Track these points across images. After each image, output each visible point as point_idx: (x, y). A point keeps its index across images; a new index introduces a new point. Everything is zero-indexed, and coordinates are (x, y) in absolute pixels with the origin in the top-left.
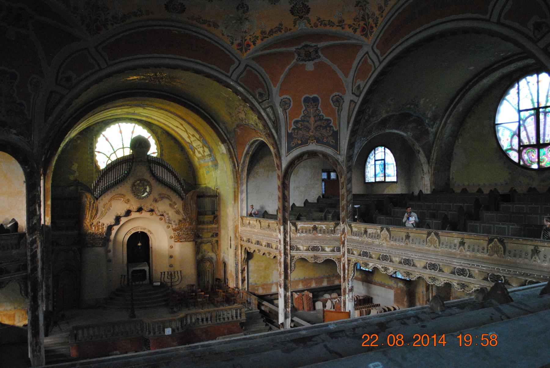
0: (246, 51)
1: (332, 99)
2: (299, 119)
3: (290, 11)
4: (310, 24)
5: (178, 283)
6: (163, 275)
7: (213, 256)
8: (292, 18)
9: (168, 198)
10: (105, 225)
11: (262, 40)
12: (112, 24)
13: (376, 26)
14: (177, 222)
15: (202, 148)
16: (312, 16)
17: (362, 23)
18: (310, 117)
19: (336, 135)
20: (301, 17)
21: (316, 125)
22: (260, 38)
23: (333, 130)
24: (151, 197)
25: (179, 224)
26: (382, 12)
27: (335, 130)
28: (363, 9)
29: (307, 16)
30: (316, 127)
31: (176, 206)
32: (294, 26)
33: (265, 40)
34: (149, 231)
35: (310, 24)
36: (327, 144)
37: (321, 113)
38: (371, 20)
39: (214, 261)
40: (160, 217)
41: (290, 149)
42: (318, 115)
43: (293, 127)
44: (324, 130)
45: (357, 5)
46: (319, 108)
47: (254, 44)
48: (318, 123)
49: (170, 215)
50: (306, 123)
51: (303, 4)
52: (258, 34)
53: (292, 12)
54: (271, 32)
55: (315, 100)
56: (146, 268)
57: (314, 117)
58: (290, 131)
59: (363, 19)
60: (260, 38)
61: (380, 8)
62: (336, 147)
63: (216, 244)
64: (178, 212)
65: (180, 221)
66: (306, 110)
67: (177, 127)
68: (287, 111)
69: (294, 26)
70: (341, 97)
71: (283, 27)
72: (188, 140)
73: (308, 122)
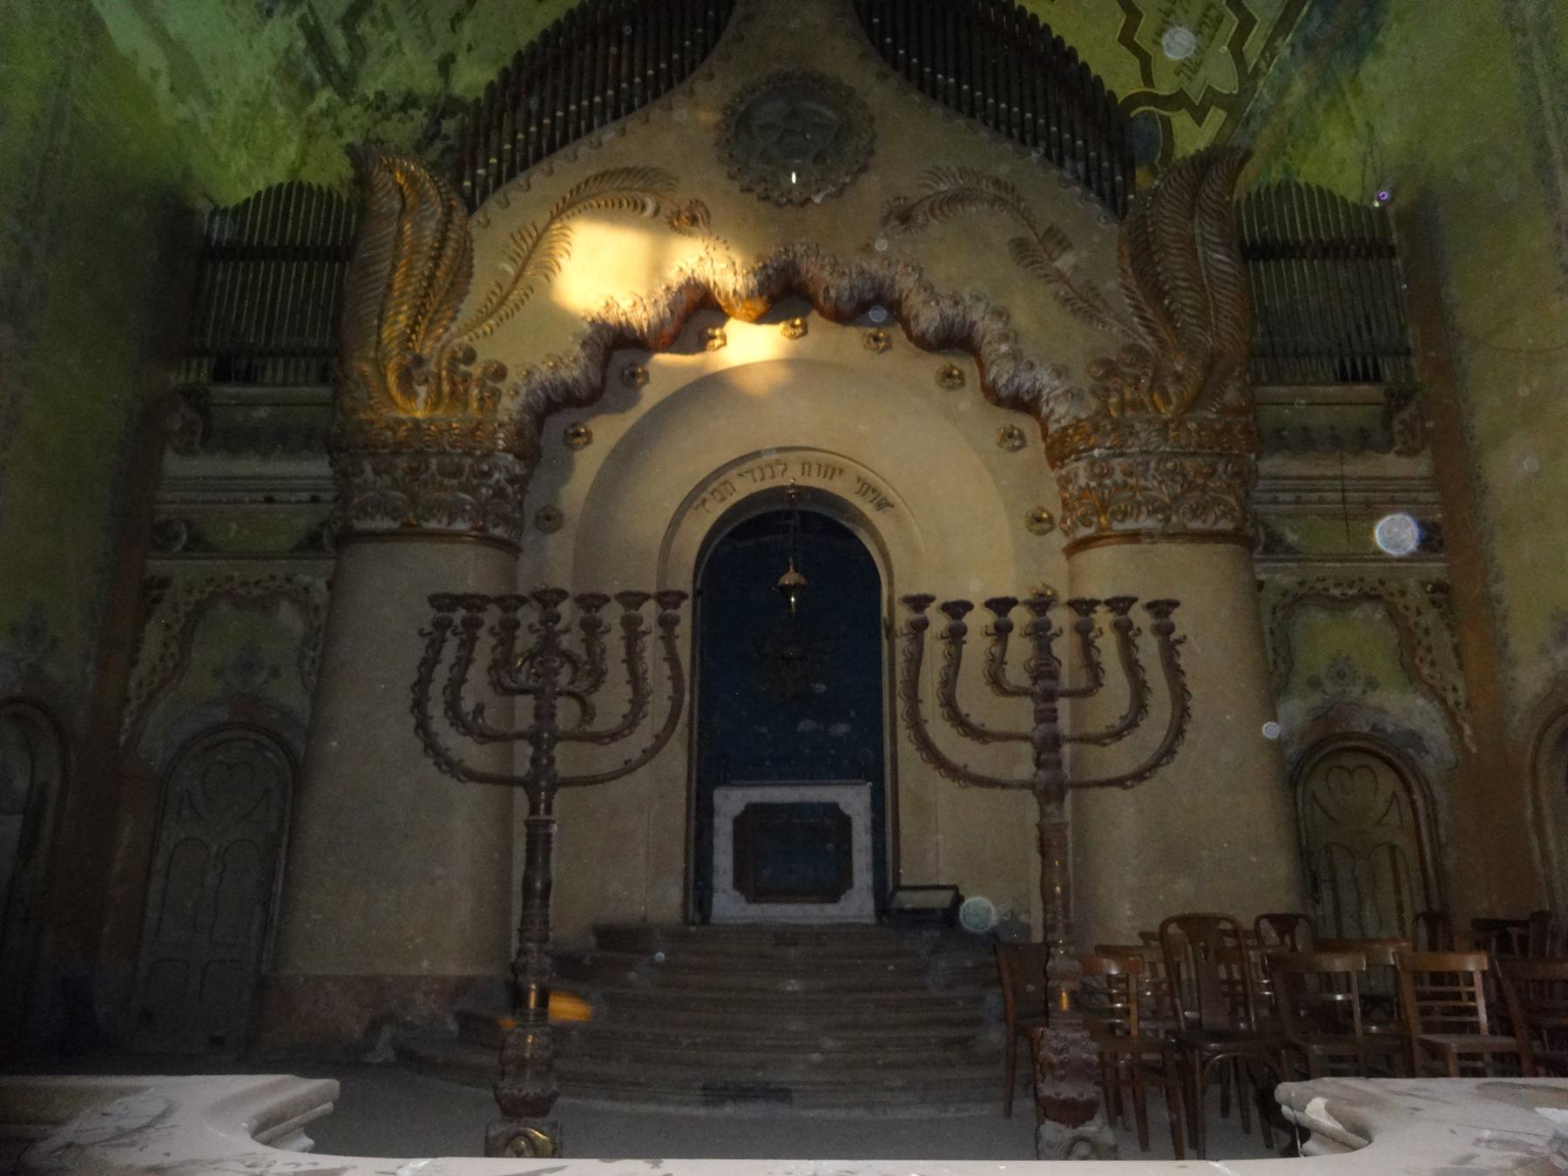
5: (1119, 759)
7: (1416, 723)
9: (1006, 196)
10: (513, 376)
14: (1082, 377)
24: (872, 190)
25: (1102, 393)
31: (1065, 262)
34: (866, 488)
39: (1429, 765)
40: (939, 362)
49: (1022, 318)
56: (853, 800)
63: (1430, 618)
64: (1083, 303)
65: (1110, 368)
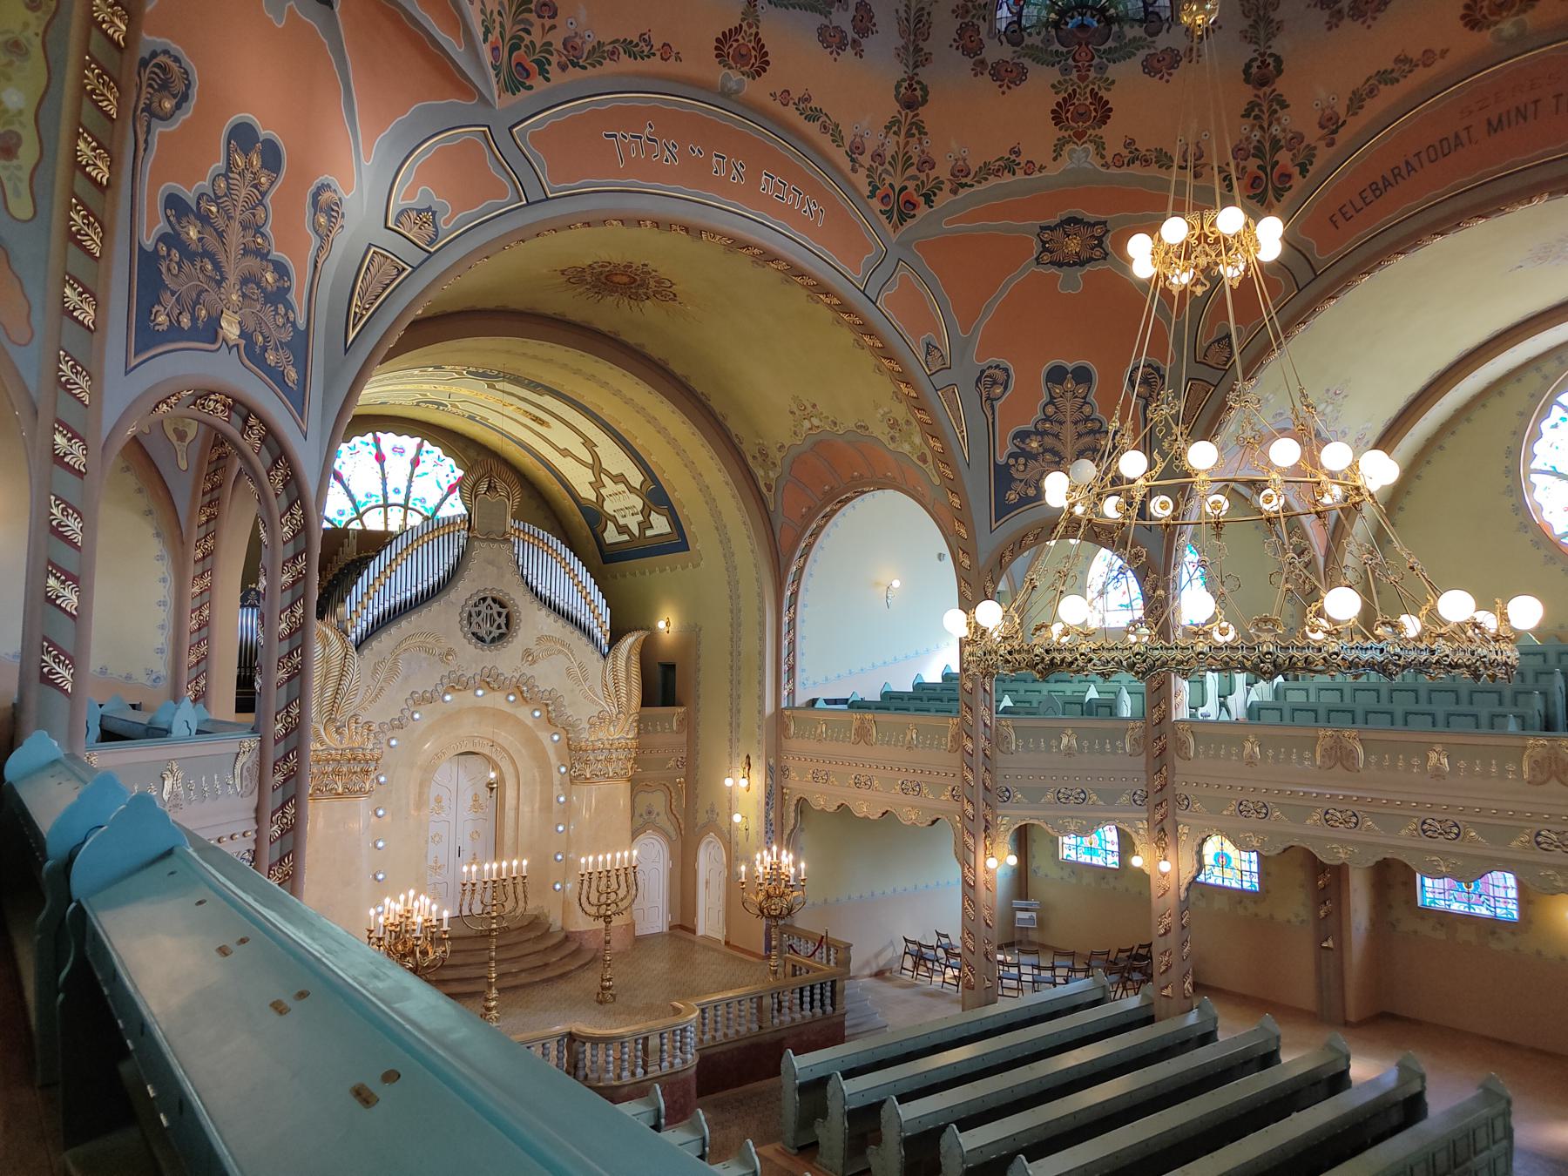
0: (902, 220)
2: (1030, 427)
3: (1053, 111)
4: (1103, 157)
6: (586, 883)
8: (1055, 133)
11: (954, 192)
12: (563, 68)
13: (1304, 171)
15: (640, 518)
16: (1113, 134)
17: (1252, 164)
18: (1061, 423)
20: (1080, 135)
22: (947, 187)
26: (1335, 132)
28: (1261, 127)
29: (1098, 132)
32: (1055, 159)
33: (963, 193)
35: (1103, 157)
37: (1097, 414)
38: (1284, 157)
42: (1088, 419)
43: (1010, 448)
45: (1246, 115)
46: (1091, 398)
47: (929, 200)
48: (1087, 439)
50: (1049, 441)
51: (1093, 94)
52: (943, 171)
53: (1057, 118)
54: (986, 171)
55: (1083, 376)
57: (1076, 423)
58: (1001, 460)
59: (1259, 152)
60: (947, 187)
61: (1331, 124)
66: (1051, 402)
67: (565, 453)
68: (997, 404)
69: (1055, 159)
71: (1022, 160)
72: (587, 493)
73: (1056, 436)
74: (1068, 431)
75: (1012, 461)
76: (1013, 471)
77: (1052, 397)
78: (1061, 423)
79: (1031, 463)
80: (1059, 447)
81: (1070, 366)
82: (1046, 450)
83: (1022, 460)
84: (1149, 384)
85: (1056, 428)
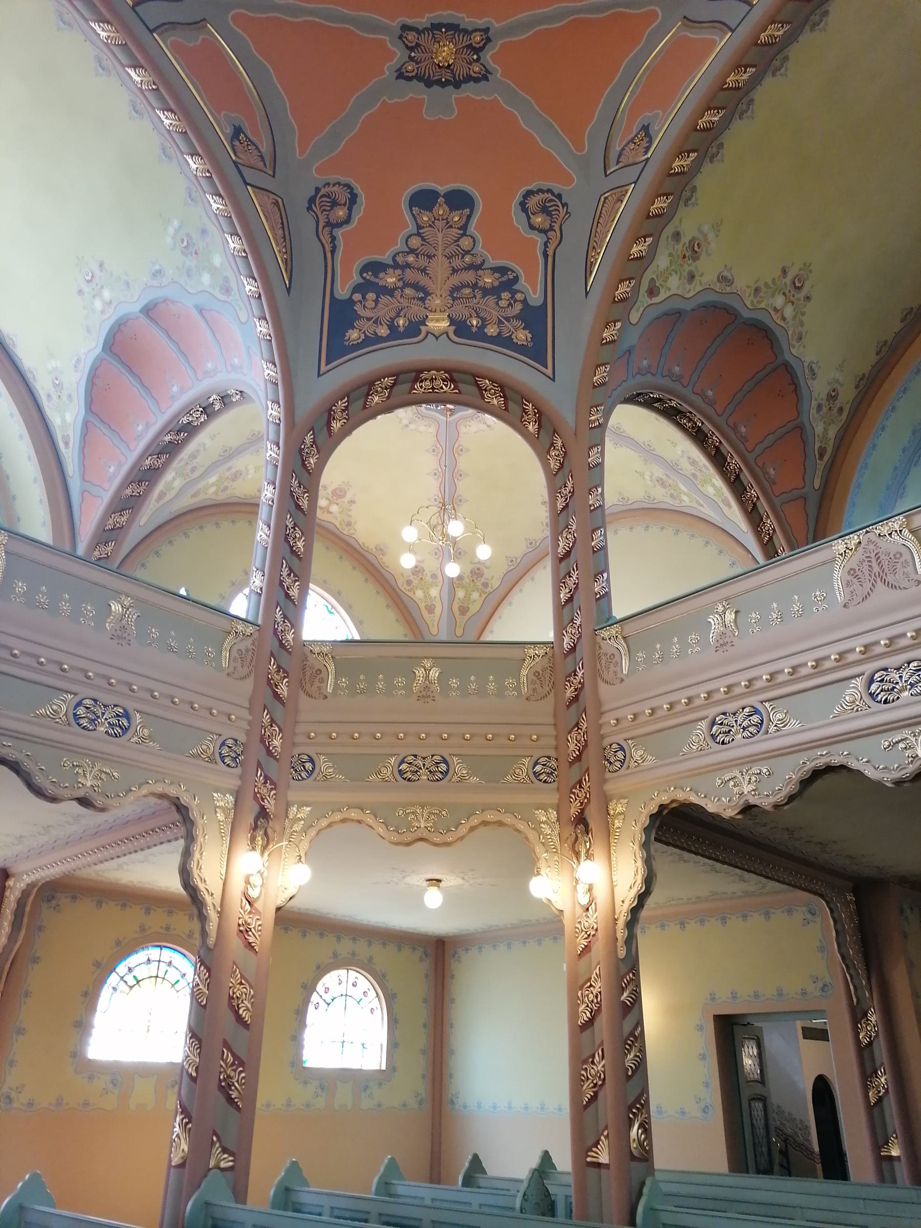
1: (523, 205)
19: (535, 318)
21: (456, 280)
23: (524, 301)
27: (535, 298)
30: (456, 289)
36: (504, 342)
41: (336, 349)
44: (491, 300)
46: (472, 229)
55: (460, 201)
58: (342, 292)
62: (537, 352)
70: (559, 197)
74: (439, 267)
75: (357, 297)
76: (358, 308)
77: (419, 227)
78: (430, 257)
79: (384, 299)
80: (424, 281)
81: (442, 189)
82: (407, 285)
83: (371, 296)
84: (549, 214)
85: (423, 262)
